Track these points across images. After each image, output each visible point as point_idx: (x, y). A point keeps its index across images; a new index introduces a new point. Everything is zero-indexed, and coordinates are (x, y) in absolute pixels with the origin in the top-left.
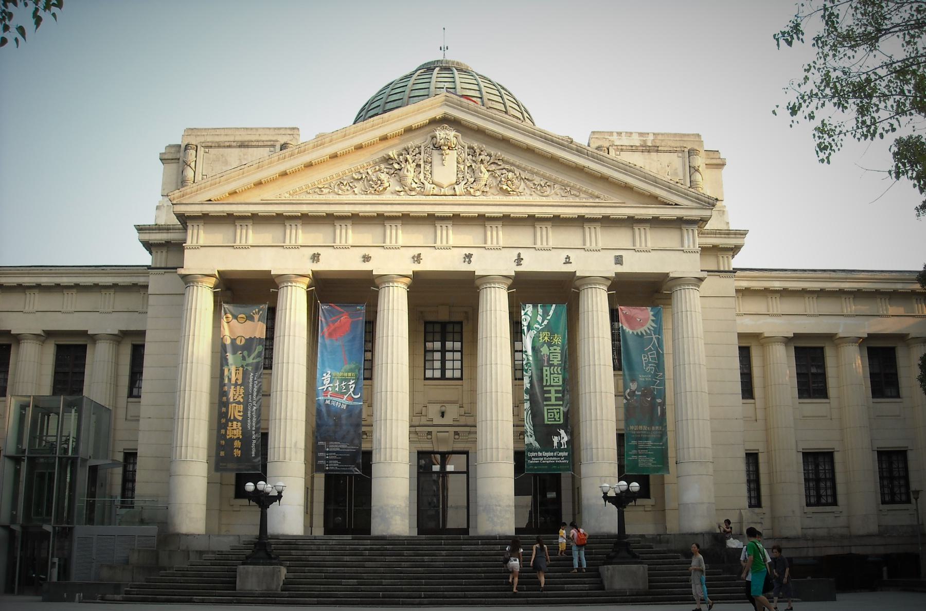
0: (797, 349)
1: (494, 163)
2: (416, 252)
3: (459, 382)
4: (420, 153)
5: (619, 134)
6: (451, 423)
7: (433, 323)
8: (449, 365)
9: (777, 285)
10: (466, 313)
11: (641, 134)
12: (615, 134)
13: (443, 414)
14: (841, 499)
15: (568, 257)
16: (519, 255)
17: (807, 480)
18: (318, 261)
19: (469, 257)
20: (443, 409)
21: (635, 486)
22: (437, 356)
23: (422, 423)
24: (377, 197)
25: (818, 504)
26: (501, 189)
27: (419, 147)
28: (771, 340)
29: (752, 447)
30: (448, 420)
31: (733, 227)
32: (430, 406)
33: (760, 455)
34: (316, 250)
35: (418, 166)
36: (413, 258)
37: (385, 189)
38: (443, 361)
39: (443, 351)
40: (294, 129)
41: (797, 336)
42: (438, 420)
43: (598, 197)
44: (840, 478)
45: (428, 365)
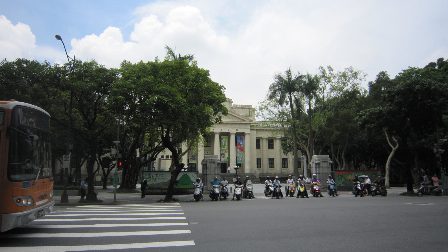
28: (264, 139)
29: (259, 157)
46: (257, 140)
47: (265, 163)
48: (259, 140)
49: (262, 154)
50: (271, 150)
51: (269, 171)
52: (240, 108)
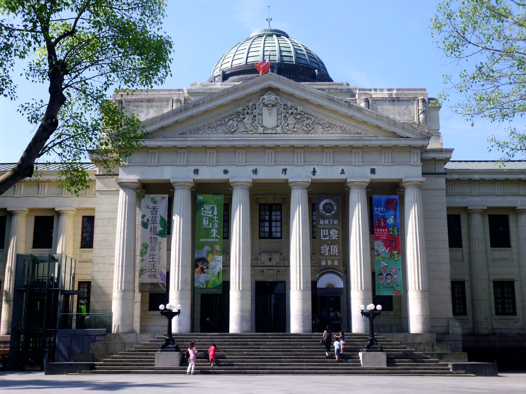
0: (490, 216)
1: (299, 114)
2: (254, 168)
3: (280, 240)
4: (255, 109)
5: (376, 90)
6: (275, 264)
7: (264, 204)
8: (274, 229)
9: (477, 177)
10: (284, 198)
11: (389, 90)
12: (373, 90)
13: (270, 260)
14: (519, 311)
15: (343, 170)
16: (314, 169)
17: (496, 298)
18: (197, 173)
19: (285, 170)
20: (270, 256)
21: (379, 307)
22: (267, 224)
23: (258, 265)
24: (231, 135)
25: (504, 313)
26: (303, 129)
27: (255, 105)
30: (273, 263)
31: (444, 147)
32: (263, 255)
33: (466, 282)
34: (196, 168)
35: (255, 116)
36: (253, 171)
37: (236, 130)
38: (270, 227)
39: (270, 221)
40: (179, 90)
41: (489, 208)
42: (268, 263)
43: (361, 133)
44: (518, 297)
45: (262, 229)
46: (449, 217)
47: (484, 297)
48: (458, 217)
49: (470, 267)
50: (500, 253)
51: (496, 325)
52: (384, 100)
